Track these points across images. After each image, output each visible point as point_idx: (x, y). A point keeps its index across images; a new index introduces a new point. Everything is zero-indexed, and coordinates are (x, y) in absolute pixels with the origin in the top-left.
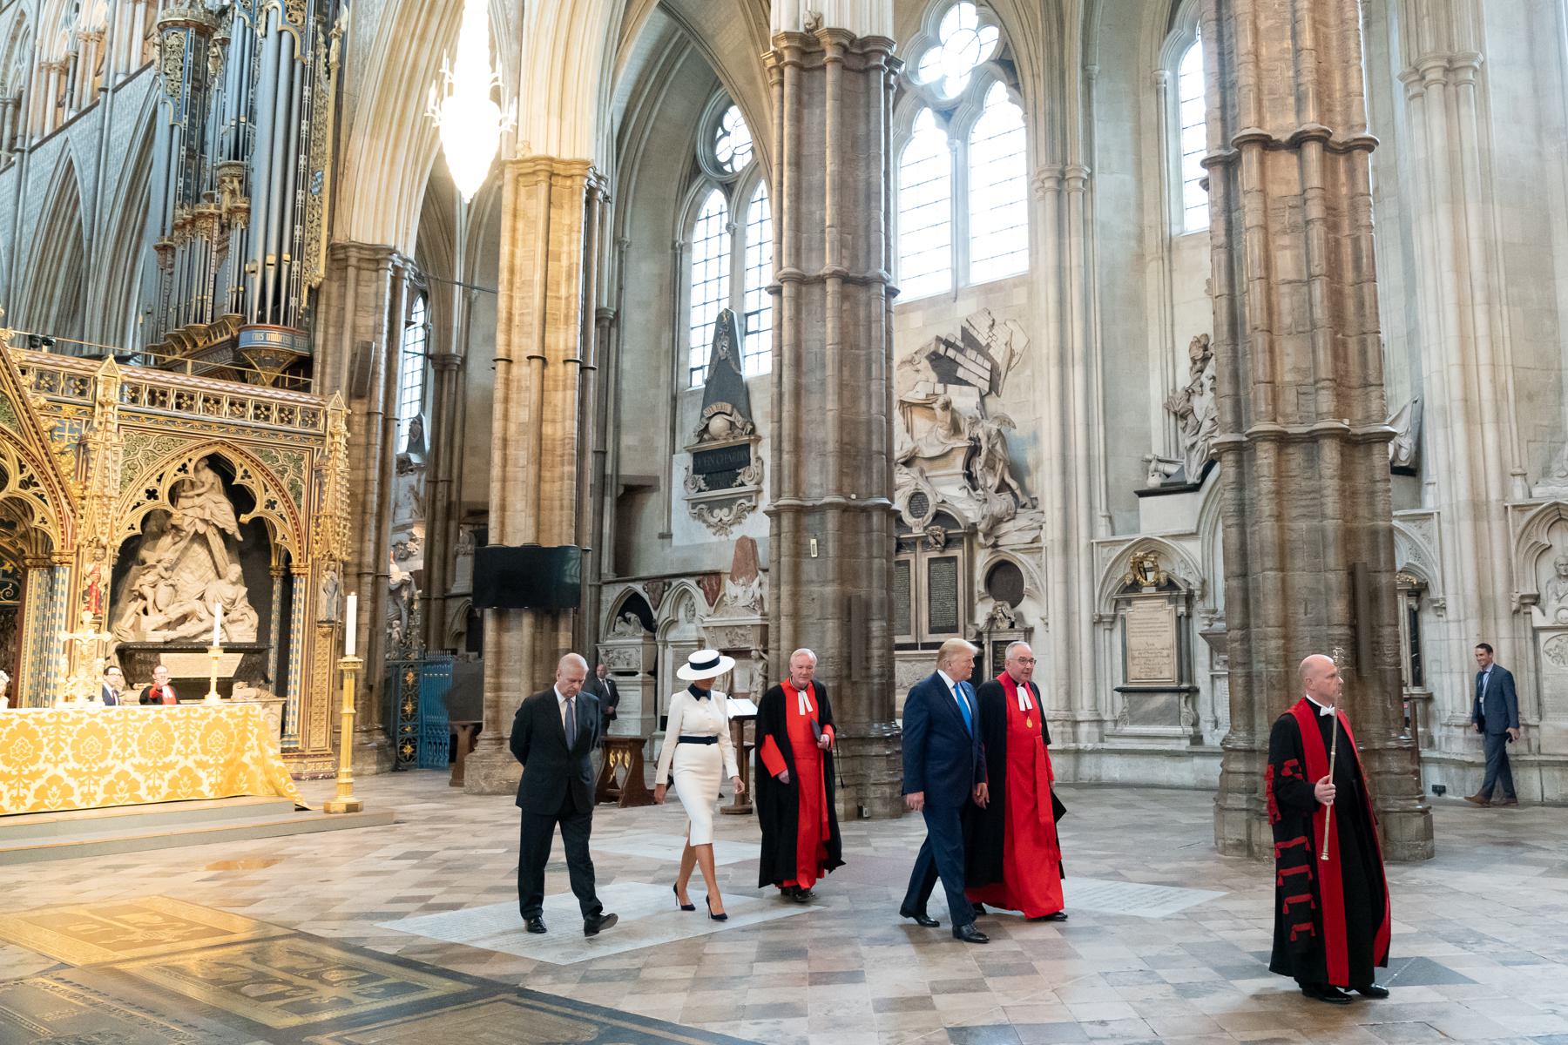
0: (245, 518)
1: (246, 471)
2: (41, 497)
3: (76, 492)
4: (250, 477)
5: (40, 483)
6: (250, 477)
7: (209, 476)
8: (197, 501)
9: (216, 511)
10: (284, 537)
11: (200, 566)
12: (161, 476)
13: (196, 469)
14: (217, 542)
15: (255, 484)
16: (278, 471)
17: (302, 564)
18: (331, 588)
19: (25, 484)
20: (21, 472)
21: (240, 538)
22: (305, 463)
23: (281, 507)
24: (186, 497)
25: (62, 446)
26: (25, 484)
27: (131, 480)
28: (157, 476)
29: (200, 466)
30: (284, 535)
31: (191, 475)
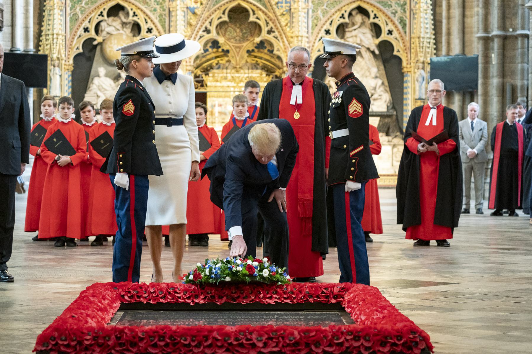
0: (377, 41)
1: (375, 15)
2: (276, 38)
3: (289, 34)
4: (377, 18)
5: (276, 31)
6: (377, 18)
7: (359, 18)
8: (354, 33)
9: (363, 38)
10: (398, 51)
11: (362, 69)
12: (332, 22)
13: (350, 14)
14: (367, 55)
15: (380, 21)
16: (392, 13)
17: (408, 66)
18: (420, 80)
19: (269, 32)
20: (267, 26)
21: (377, 52)
22: (407, 7)
23: (395, 34)
24: (349, 31)
25: (282, 11)
26: (269, 32)
27: (316, 25)
28: (329, 22)
29: (354, 13)
30: (399, 50)
31: (347, 20)
